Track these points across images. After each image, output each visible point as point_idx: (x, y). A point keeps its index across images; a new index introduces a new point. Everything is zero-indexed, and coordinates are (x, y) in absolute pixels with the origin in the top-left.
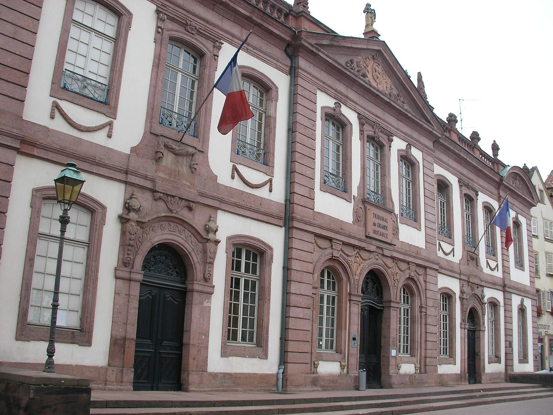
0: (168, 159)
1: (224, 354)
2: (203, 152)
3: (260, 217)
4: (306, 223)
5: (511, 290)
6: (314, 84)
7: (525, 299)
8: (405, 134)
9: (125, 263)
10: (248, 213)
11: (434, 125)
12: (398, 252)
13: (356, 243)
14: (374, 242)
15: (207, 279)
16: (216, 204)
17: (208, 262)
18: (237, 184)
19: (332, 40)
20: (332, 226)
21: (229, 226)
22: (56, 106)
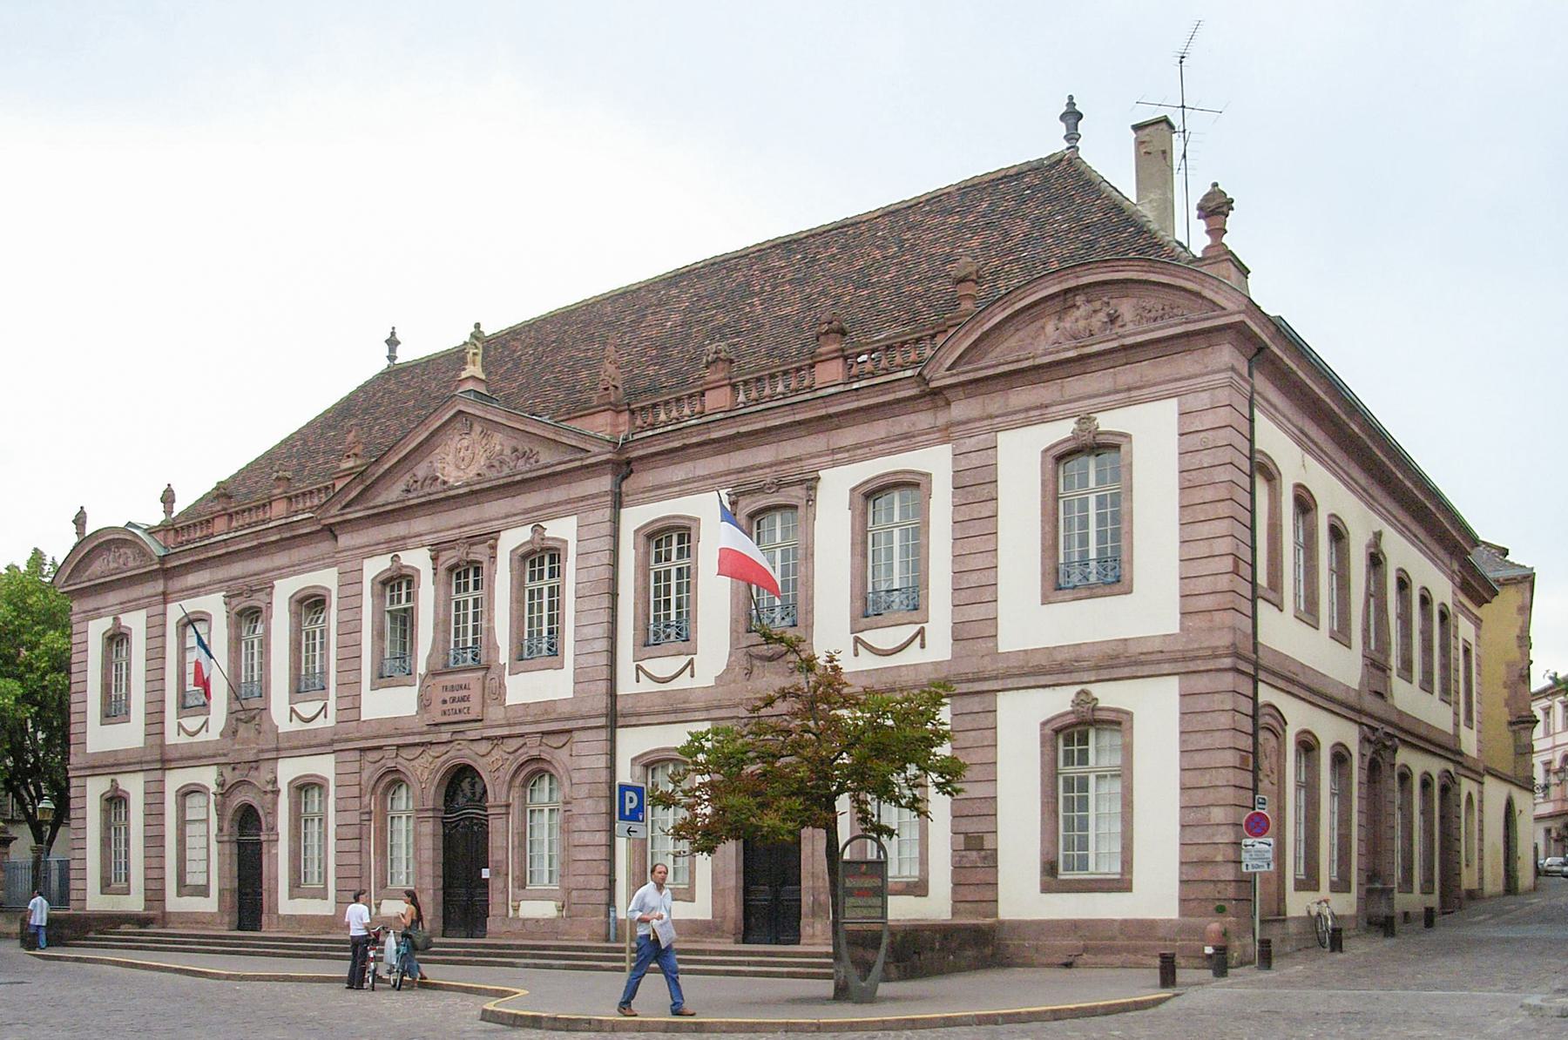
0: (242, 728)
1: (291, 897)
2: (266, 709)
3: (314, 750)
4: (347, 741)
5: (986, 686)
6: (355, 556)
7: (1097, 690)
8: (526, 512)
9: (220, 829)
10: (303, 752)
11: (588, 447)
12: (492, 727)
13: (417, 739)
14: (443, 728)
15: (273, 829)
16: (273, 755)
17: (273, 812)
18: (297, 726)
19: (363, 481)
20: (384, 731)
21: (288, 770)
22: (180, 725)
